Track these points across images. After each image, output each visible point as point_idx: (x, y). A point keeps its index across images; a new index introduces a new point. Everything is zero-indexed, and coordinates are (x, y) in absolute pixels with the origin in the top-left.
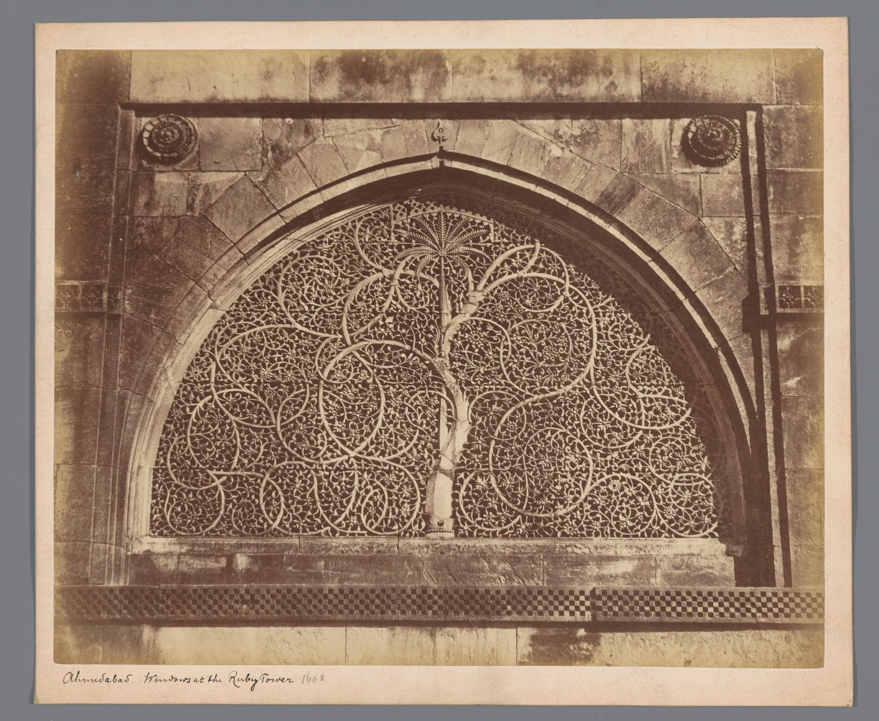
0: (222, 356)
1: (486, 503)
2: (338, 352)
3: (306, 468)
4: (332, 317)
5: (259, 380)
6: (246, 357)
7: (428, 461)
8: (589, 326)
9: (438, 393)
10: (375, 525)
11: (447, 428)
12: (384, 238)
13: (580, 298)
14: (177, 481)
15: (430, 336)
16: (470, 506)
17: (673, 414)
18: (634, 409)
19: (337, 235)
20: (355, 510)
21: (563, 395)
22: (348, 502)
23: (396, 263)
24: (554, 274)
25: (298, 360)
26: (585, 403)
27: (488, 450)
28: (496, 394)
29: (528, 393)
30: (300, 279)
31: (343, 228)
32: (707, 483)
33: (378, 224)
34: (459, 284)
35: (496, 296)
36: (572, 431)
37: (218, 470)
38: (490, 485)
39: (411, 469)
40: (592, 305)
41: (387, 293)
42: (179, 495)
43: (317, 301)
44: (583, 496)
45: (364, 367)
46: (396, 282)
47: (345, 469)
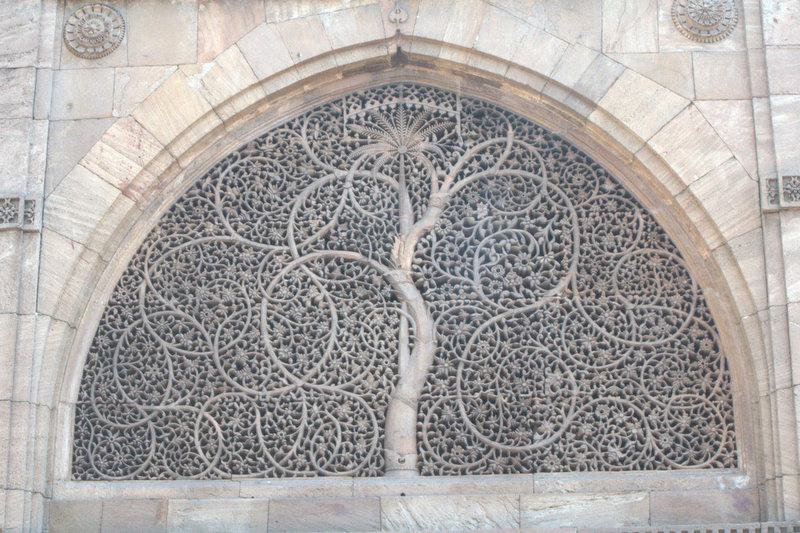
0: (153, 274)
1: (454, 437)
2: (284, 266)
3: (248, 401)
4: (277, 227)
6: (180, 275)
10: (327, 463)
14: (102, 418)
15: (388, 245)
16: (435, 440)
19: (283, 133)
20: (303, 448)
21: (542, 308)
22: (295, 438)
23: (349, 163)
24: (530, 170)
25: (238, 277)
26: (567, 317)
27: (455, 374)
29: (501, 307)
32: (707, 406)
37: (149, 404)
38: (458, 415)
39: (368, 399)
40: (573, 204)
41: (339, 197)
42: (105, 434)
43: (260, 209)
44: (564, 427)
45: (312, 283)
46: (348, 184)
47: (292, 400)
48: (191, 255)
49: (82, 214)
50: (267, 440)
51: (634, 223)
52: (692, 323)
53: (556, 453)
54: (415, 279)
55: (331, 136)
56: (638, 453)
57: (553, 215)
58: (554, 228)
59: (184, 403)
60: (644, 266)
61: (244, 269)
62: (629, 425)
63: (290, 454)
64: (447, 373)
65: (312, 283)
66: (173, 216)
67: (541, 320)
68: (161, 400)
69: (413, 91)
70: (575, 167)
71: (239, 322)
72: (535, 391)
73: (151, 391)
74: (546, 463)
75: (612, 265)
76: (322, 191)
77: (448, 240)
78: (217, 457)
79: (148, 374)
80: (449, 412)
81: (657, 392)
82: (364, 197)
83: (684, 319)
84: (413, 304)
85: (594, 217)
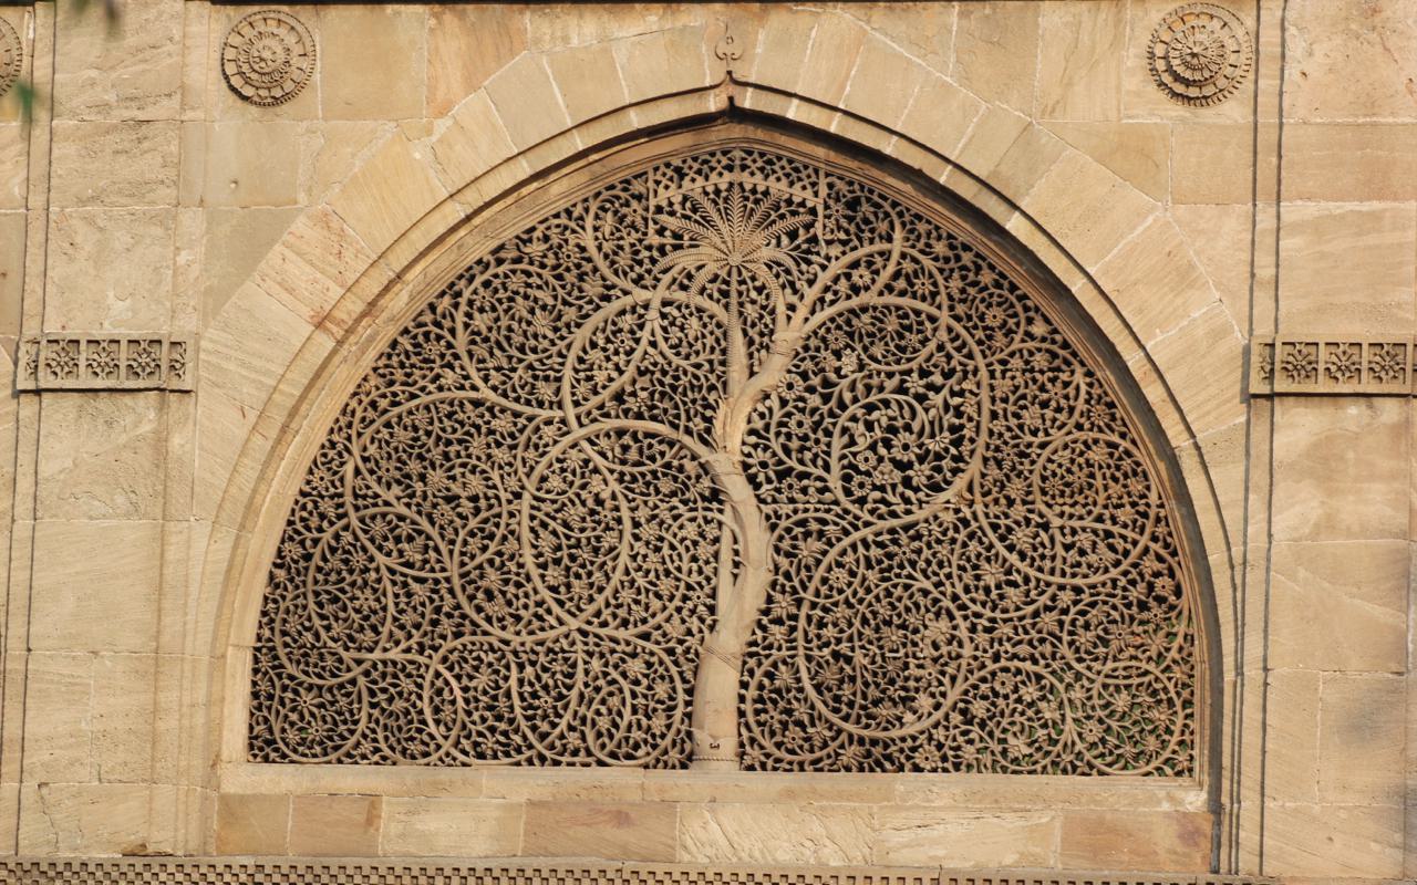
0: (365, 449)
1: (789, 712)
2: (556, 442)
3: (500, 649)
4: (547, 379)
5: (425, 492)
6: (405, 451)
7: (698, 636)
8: (976, 395)
9: (718, 516)
10: (610, 746)
11: (732, 579)
12: (637, 231)
13: (964, 344)
14: (291, 669)
15: (709, 413)
16: (763, 717)
17: (1113, 556)
18: (1045, 547)
19: (558, 226)
21: (927, 521)
22: (566, 707)
24: (924, 299)
25: (489, 456)
26: (961, 537)
27: (794, 618)
28: (817, 519)
29: (867, 517)
30: (494, 309)
31: (569, 213)
32: (1157, 679)
33: (627, 204)
34: (761, 317)
35: (824, 340)
36: (938, 585)
38: (798, 680)
39: (671, 652)
40: (985, 357)
42: (296, 692)
43: (522, 349)
44: (947, 703)
45: (596, 470)
46: (653, 314)
47: (563, 651)
48: (421, 417)
49: (257, 362)
50: (525, 709)
51: (1071, 391)
52: (1146, 550)
53: (934, 743)
54: (746, 467)
55: (629, 234)
56: (1050, 748)
57: (953, 372)
58: (953, 394)
59: (408, 650)
60: (1081, 460)
61: (499, 445)
62: (1043, 705)
63: (557, 731)
64: (784, 617)
65: (596, 470)
66: (395, 358)
67: (924, 539)
68: (376, 643)
69: (754, 161)
70: (991, 295)
71: (489, 527)
72: (910, 649)
73: (361, 629)
74: (919, 758)
75: (1034, 456)
76: (614, 323)
77: (796, 407)
78: (454, 733)
79: (357, 604)
80: (785, 676)
81: (1085, 656)
82: (675, 333)
83: (1135, 543)
84: (741, 509)
85: (1013, 378)
